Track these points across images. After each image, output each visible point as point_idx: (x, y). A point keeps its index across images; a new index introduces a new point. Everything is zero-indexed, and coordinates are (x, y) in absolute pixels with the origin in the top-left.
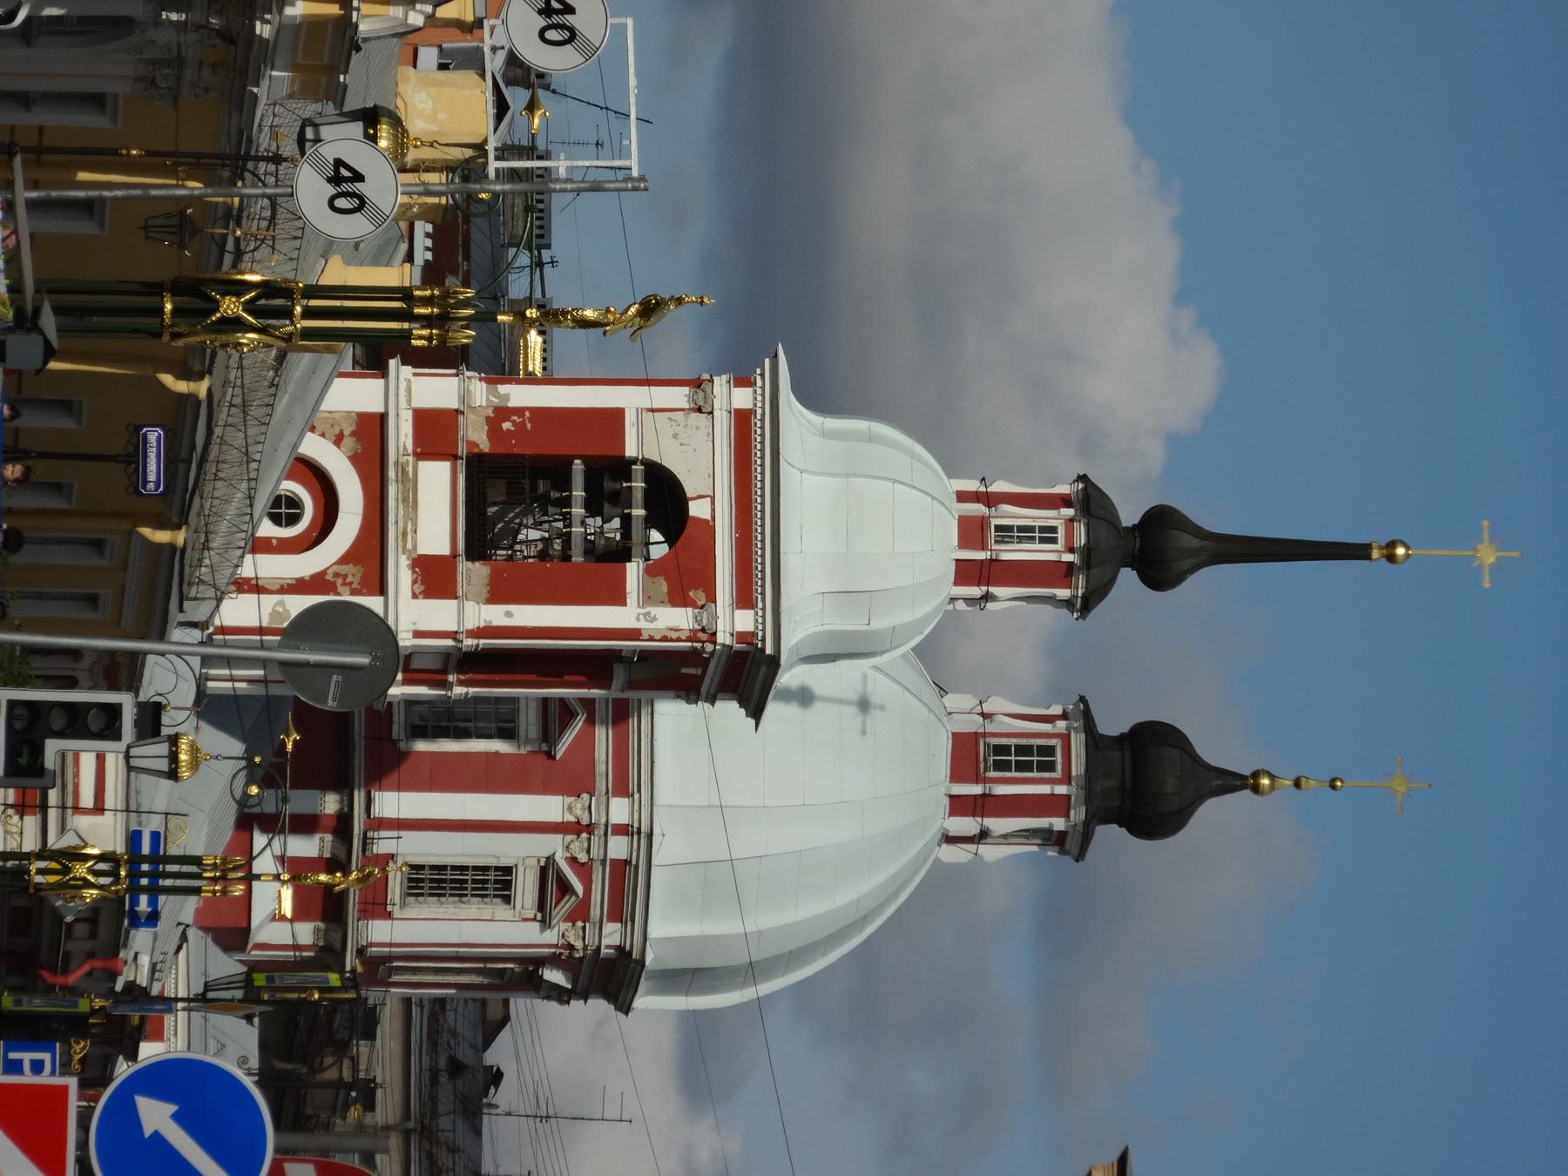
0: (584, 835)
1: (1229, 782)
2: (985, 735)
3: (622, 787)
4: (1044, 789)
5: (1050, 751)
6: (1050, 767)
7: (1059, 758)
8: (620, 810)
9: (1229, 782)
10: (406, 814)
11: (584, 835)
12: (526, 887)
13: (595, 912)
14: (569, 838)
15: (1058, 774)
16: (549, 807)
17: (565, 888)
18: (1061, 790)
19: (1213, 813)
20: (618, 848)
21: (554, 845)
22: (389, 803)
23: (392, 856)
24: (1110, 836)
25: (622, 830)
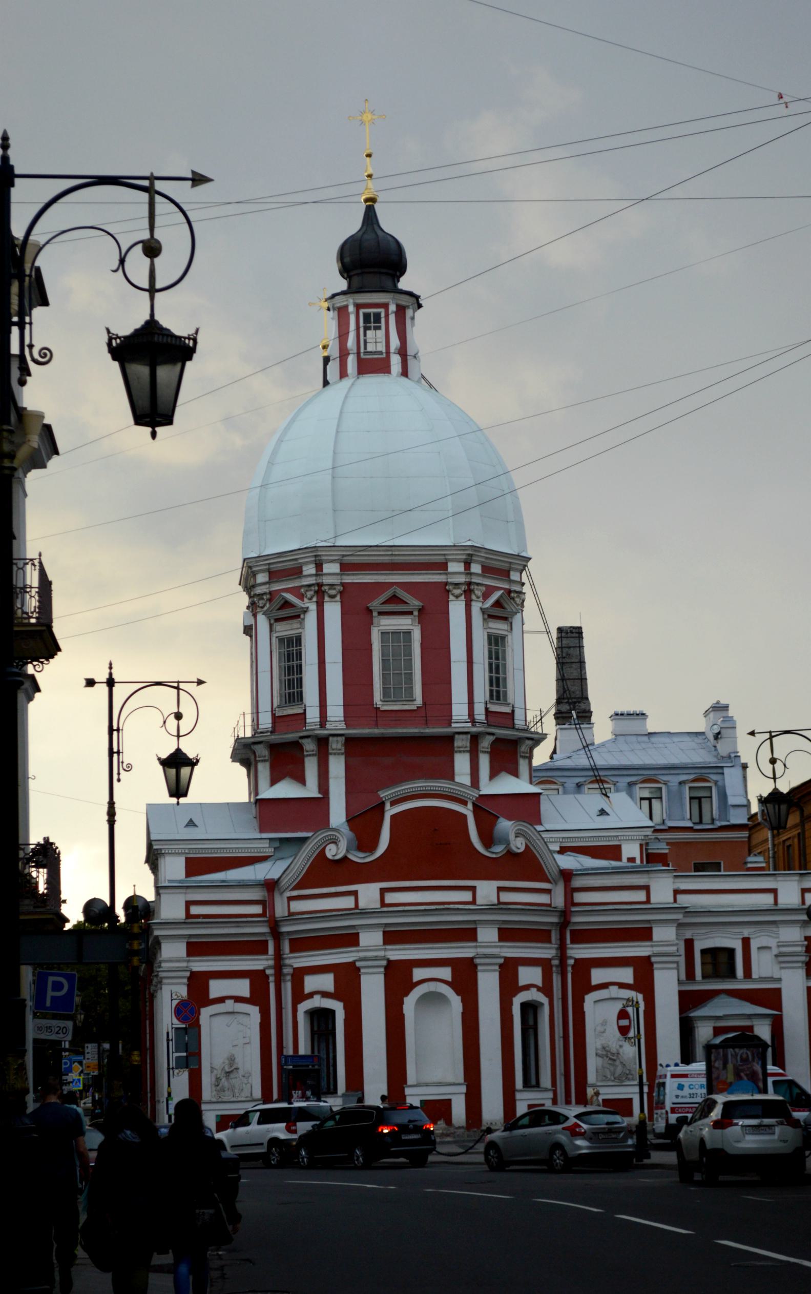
0: (472, 587)
1: (370, 217)
2: (358, 353)
3: (442, 566)
4: (392, 318)
5: (367, 317)
6: (377, 317)
7: (372, 311)
8: (455, 567)
9: (370, 217)
10: (465, 699)
11: (472, 587)
12: (499, 627)
13: (507, 586)
14: (474, 597)
15: (382, 311)
16: (456, 609)
17: (498, 604)
18: (392, 308)
19: (389, 223)
20: (476, 568)
21: (476, 607)
22: (459, 711)
23: (486, 709)
24: (404, 283)
25: (467, 565)
